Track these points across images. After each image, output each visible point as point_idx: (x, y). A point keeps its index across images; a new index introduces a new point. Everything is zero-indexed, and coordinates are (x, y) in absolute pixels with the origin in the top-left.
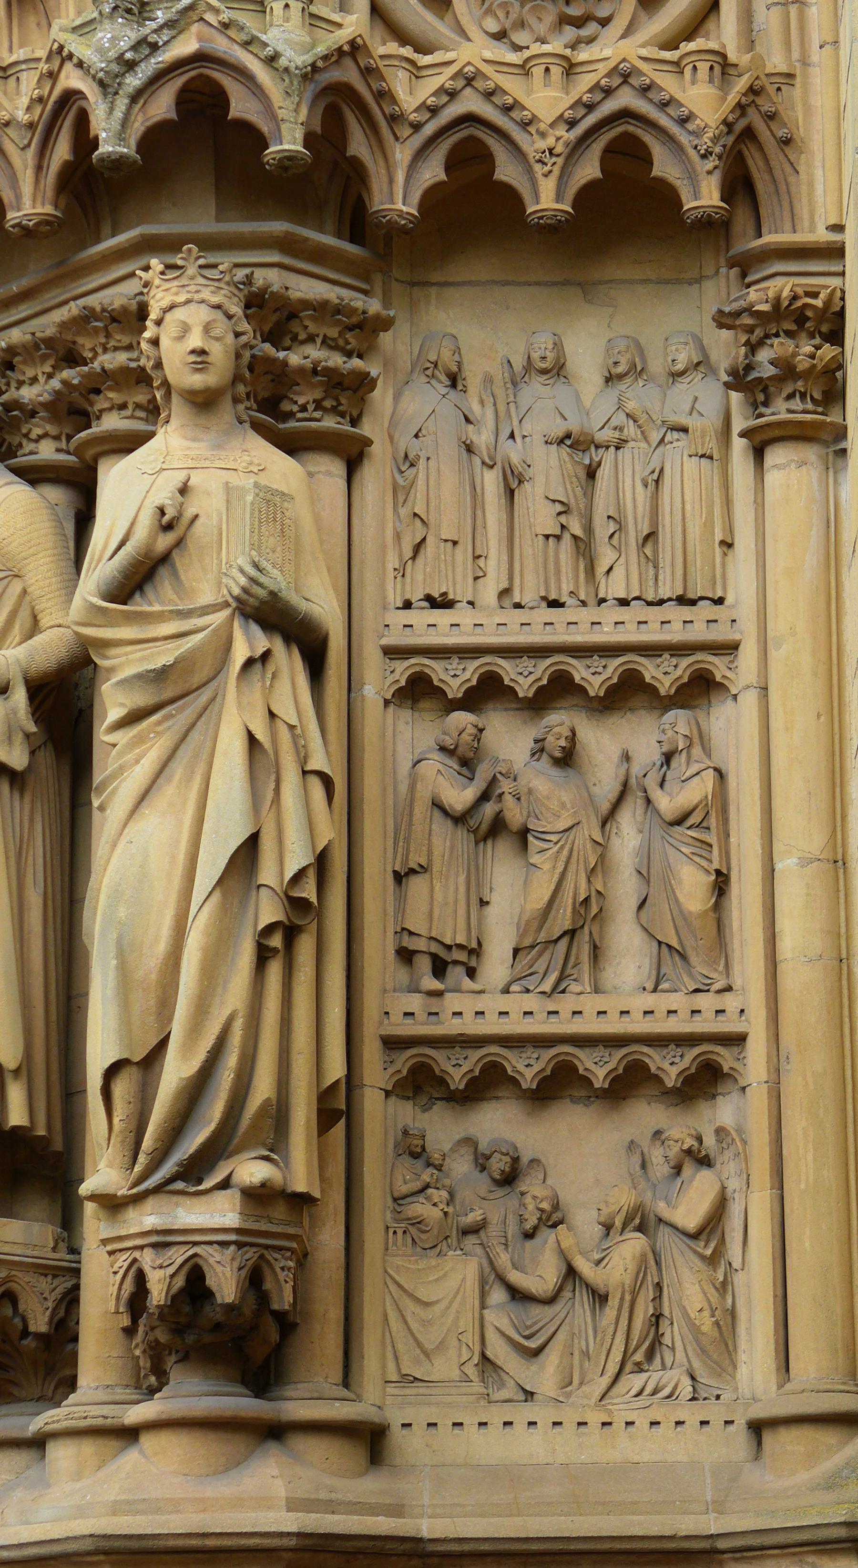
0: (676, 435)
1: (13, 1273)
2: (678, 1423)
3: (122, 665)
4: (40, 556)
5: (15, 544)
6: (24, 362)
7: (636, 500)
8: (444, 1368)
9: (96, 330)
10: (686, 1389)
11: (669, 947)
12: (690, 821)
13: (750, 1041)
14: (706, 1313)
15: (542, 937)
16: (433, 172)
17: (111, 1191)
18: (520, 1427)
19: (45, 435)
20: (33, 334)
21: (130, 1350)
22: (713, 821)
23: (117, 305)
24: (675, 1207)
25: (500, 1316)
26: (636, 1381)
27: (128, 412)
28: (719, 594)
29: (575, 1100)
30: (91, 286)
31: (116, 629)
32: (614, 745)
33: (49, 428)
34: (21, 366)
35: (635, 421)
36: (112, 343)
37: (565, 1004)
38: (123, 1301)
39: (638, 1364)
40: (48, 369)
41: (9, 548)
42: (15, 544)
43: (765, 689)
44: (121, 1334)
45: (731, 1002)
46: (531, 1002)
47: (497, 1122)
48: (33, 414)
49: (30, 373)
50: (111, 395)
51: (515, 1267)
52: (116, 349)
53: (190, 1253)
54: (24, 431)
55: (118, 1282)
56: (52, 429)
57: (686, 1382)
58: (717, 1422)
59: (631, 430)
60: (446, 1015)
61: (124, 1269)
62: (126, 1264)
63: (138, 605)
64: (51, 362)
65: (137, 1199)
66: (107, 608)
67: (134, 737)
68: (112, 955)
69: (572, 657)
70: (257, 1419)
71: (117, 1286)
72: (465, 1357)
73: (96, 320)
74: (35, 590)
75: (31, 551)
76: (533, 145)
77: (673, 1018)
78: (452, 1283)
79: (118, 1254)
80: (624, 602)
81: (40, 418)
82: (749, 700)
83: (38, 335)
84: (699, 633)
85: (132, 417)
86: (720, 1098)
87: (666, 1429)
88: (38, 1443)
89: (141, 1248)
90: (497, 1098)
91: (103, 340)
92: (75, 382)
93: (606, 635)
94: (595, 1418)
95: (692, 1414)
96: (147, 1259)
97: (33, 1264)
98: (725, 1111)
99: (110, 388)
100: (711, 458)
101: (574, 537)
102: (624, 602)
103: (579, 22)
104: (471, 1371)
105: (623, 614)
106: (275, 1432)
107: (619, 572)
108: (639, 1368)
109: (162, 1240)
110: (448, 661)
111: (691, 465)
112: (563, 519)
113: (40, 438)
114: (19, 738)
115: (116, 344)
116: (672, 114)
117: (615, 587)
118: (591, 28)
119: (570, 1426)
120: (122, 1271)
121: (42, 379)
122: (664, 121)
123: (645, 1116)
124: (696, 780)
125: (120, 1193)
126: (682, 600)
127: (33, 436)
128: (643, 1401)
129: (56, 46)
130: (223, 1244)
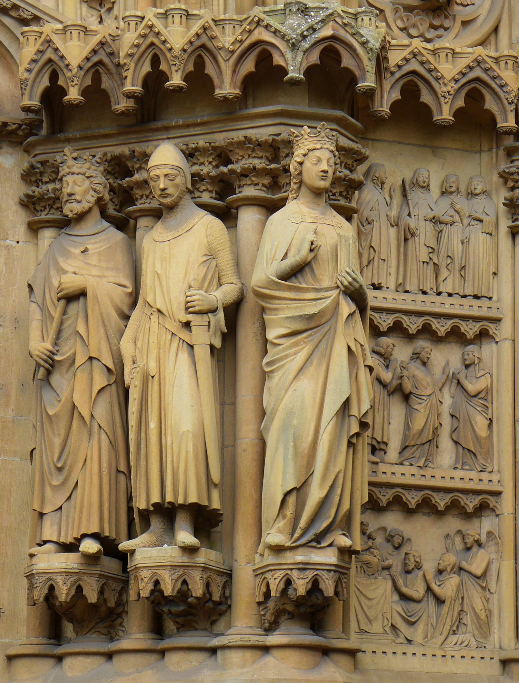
0: (476, 222)
1: (186, 571)
2: (472, 657)
3: (282, 309)
4: (225, 250)
5: (215, 244)
6: (200, 155)
7: (457, 248)
8: (377, 627)
9: (248, 148)
10: (474, 643)
11: (468, 450)
12: (480, 396)
13: (504, 495)
14: (483, 611)
15: (419, 442)
16: (396, 95)
17: (283, 544)
18: (409, 655)
19: (207, 190)
20: (210, 143)
21: (259, 611)
22: (490, 396)
23: (263, 138)
24: (471, 565)
25: (399, 607)
26: (454, 639)
27: (257, 187)
28: (491, 296)
29: (424, 514)
30: (243, 126)
31: (282, 292)
32: (446, 358)
33: (209, 187)
34: (199, 157)
35: (458, 214)
36: (254, 155)
37: (428, 472)
38: (278, 592)
39: (454, 631)
40: (211, 160)
41: (213, 245)
42: (215, 244)
43: (514, 341)
44: (256, 605)
45: (495, 477)
46: (414, 470)
47: (392, 521)
48: (203, 180)
49: (201, 160)
50: (253, 179)
51: (406, 586)
52: (255, 157)
53: (315, 573)
54: (197, 187)
55: (277, 583)
56: (210, 188)
57: (473, 639)
58: (487, 658)
59: (457, 218)
60: (379, 473)
61: (281, 578)
62: (282, 576)
63: (293, 282)
65: (291, 549)
66: (280, 283)
67: (293, 343)
68: (291, 440)
69: (433, 318)
70: (320, 645)
71: (276, 585)
72: (385, 624)
73: (249, 143)
74: (222, 266)
75: (222, 248)
76: (440, 89)
77: (471, 482)
78: (380, 591)
79: (277, 571)
80: (450, 295)
81: (206, 182)
82: (507, 346)
83: (212, 144)
84: (484, 312)
85: (260, 190)
86: (483, 518)
87: (399, 655)
88: (213, 651)
89: (291, 569)
90: (392, 510)
91: (250, 153)
92: (238, 171)
93: (447, 309)
94: (439, 653)
95: (419, 651)
96: (295, 574)
97: (218, 571)
98: (487, 524)
99: (253, 176)
100: (491, 234)
101: (434, 263)
102: (450, 295)
103: (436, 28)
104: (388, 629)
105: (450, 300)
106: (326, 652)
107: (450, 281)
108: (454, 633)
109: (304, 567)
110: (381, 314)
111: (483, 237)
112: (431, 255)
113: (204, 190)
114: (219, 333)
115: (256, 155)
116: (497, 82)
117: (447, 287)
118: (441, 32)
119: (429, 656)
120: (279, 579)
121: (206, 164)
122: (494, 85)
123: (453, 524)
124: (483, 377)
125: (286, 545)
126: (476, 297)
127: (201, 189)
128: (457, 647)
130: (329, 571)
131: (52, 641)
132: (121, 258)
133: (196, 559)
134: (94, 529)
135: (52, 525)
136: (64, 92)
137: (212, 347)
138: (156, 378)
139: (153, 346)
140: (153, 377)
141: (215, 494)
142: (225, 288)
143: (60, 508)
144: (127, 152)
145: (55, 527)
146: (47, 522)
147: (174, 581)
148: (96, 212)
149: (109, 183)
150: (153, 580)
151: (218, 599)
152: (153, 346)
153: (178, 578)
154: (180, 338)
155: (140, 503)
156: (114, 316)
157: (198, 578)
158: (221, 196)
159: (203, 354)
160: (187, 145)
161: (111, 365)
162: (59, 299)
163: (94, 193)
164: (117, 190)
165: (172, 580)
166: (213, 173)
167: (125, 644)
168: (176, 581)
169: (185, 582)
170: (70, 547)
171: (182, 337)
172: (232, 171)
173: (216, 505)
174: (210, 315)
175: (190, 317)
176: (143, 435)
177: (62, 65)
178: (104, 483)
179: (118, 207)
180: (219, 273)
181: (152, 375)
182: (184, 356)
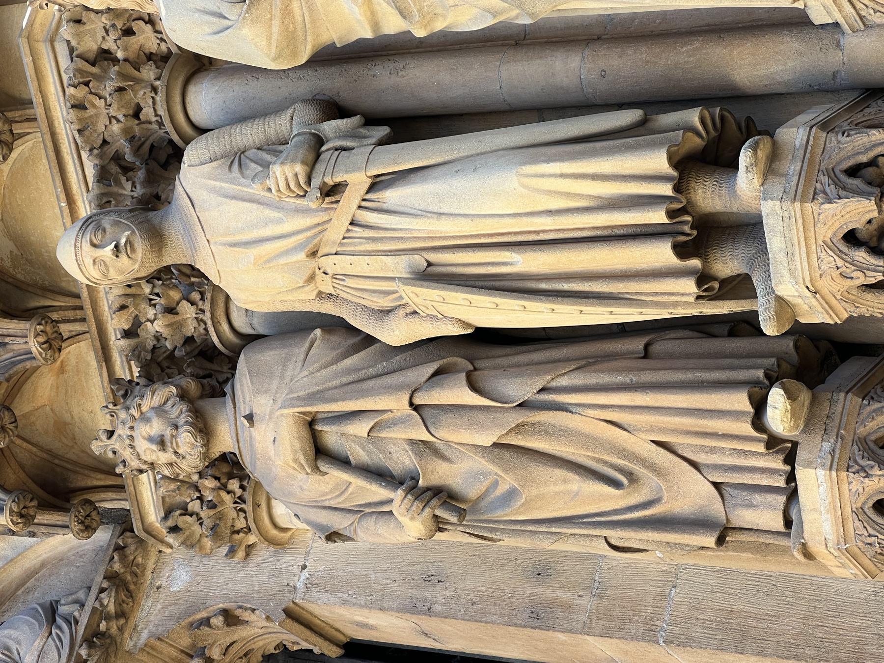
64: (123, 179)
114: (363, 131)
133: (798, 144)
134: (740, 401)
135: (751, 506)
138: (433, 257)
140: (430, 264)
143: (716, 485)
144: (123, 343)
145: (758, 498)
146: (745, 517)
147: (842, 193)
150: (845, 249)
153: (837, 183)
154: (360, 207)
157: (844, 139)
165: (840, 198)
168: (844, 189)
169: (854, 171)
171: (356, 202)
176: (543, 286)
178: (654, 379)
180: (274, 144)
181: (425, 264)
182: (391, 196)
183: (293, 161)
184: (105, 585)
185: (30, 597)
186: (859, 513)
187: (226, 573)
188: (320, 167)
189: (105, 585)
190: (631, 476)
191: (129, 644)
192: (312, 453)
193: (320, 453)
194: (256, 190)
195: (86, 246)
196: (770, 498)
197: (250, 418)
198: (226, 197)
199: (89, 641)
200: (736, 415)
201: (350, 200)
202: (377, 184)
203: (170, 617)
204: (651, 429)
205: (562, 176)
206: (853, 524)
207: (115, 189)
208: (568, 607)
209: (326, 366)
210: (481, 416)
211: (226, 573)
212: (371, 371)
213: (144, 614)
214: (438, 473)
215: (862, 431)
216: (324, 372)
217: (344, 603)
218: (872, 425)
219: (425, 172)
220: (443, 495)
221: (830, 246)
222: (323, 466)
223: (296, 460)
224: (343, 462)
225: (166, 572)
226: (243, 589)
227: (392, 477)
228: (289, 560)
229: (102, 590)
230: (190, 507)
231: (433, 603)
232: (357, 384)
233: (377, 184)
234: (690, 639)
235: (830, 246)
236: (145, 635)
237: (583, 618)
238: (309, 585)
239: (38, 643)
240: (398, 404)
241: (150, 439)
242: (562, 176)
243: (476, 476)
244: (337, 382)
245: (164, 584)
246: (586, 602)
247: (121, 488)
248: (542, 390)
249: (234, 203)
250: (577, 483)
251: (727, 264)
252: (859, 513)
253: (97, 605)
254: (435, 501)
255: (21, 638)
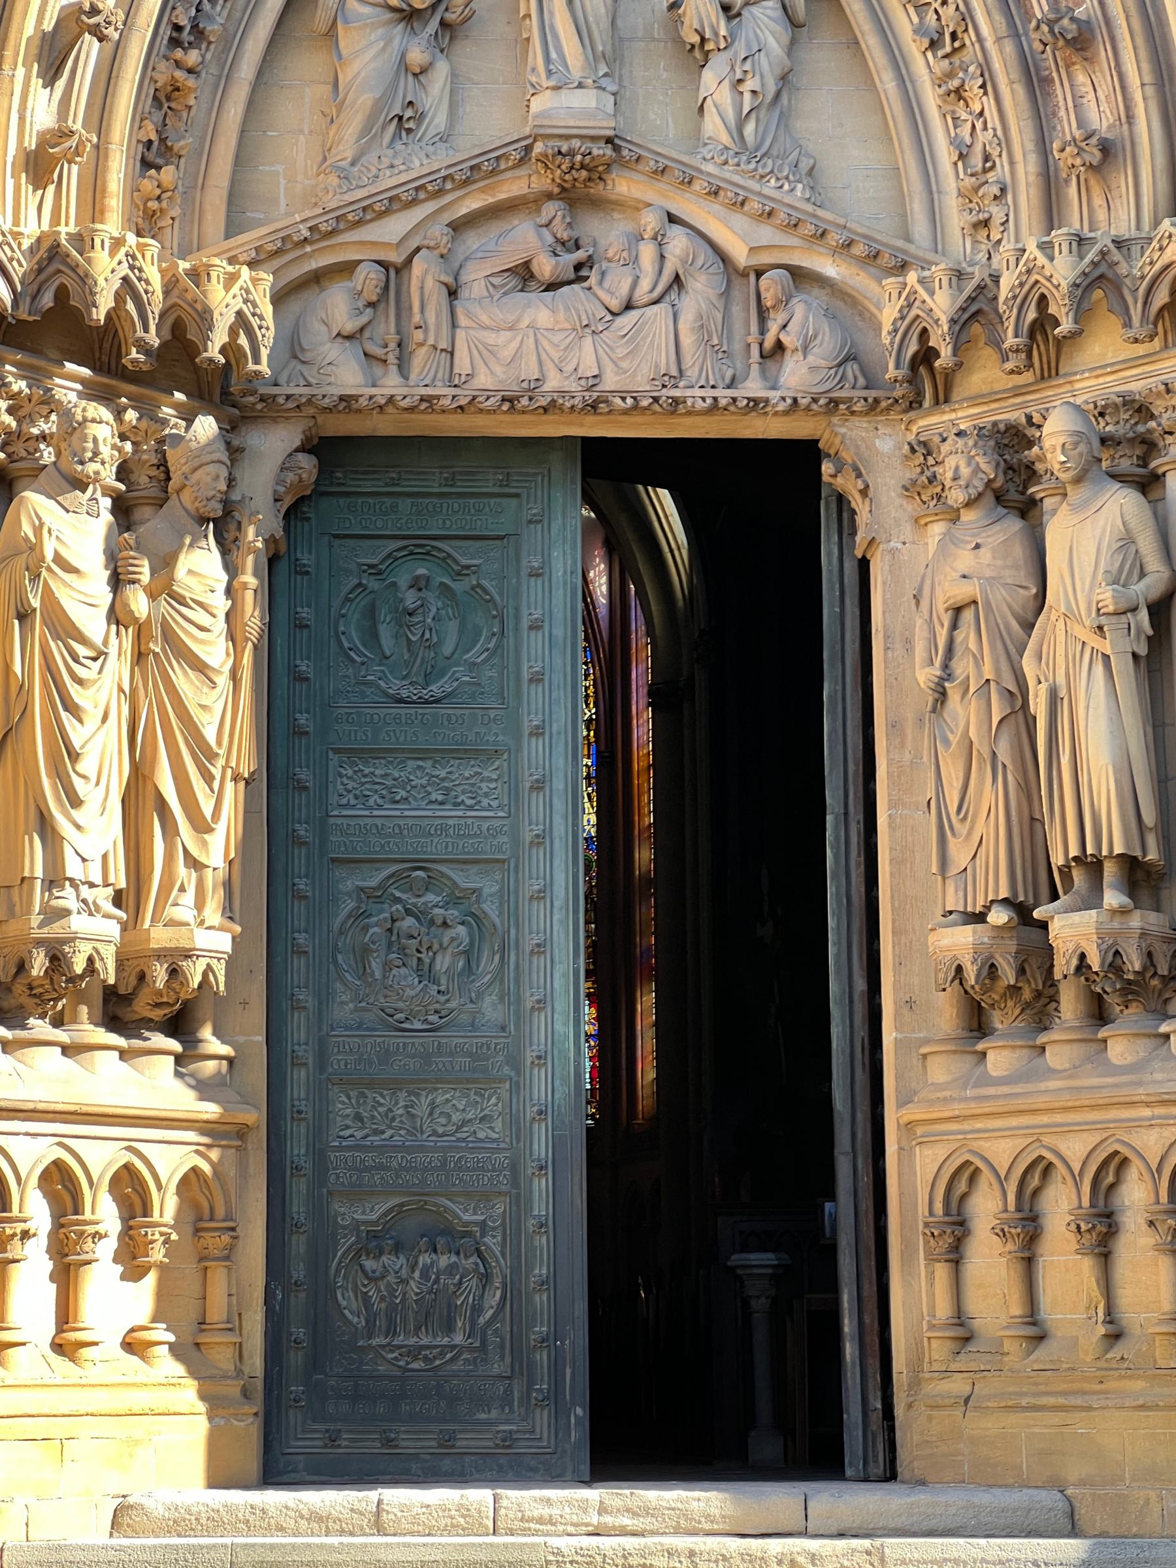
114: (1143, 637)
121: (1122, 423)
129: (1167, 234)
131: (975, 1034)
132: (1019, 551)
134: (1004, 893)
135: (956, 891)
136: (937, 355)
137: (1135, 656)
138: (1066, 701)
139: (1061, 660)
141: (1151, 841)
142: (1146, 581)
145: (961, 894)
146: (951, 888)
148: (989, 498)
149: (1005, 461)
151: (1166, 973)
152: (1061, 660)
153: (1109, 948)
155: (1058, 860)
156: (1015, 625)
158: (1144, 461)
159: (1123, 668)
160: (1095, 403)
161: (1012, 687)
162: (947, 610)
163: (983, 476)
164: (1016, 467)
166: (1131, 435)
167: (1053, 1035)
170: (979, 918)
171: (1096, 647)
172: (1150, 431)
173: (1152, 855)
174: (1129, 615)
175: (1103, 620)
177: (931, 321)
179: (1020, 488)
182: (1099, 669)
183: (1116, 604)
184: (870, 400)
185: (857, 318)
186: (955, 958)
187: (893, 482)
188: (1114, 619)
189: (870, 400)
190: (965, 818)
191: (835, 420)
192: (959, 605)
193: (958, 610)
194: (1100, 577)
195: (1062, 440)
196: (962, 902)
197: (977, 546)
198: (1099, 544)
199: (831, 400)
200: (997, 891)
201: (1094, 641)
202: (1106, 658)
203: (857, 447)
204: (988, 834)
205: (1108, 791)
206: (949, 955)
207: (1122, 410)
208: (902, 745)
209: (1010, 607)
210: (986, 727)
211: (893, 482)
212: (1008, 642)
213: (857, 424)
214: (954, 696)
215: (997, 956)
216: (1006, 609)
217: (884, 583)
218: (1001, 960)
219: (1113, 697)
220: (942, 695)
221: (1078, 946)
222: (950, 612)
223: (949, 598)
224: (954, 626)
225: (888, 431)
226: (884, 499)
227: (950, 659)
228: (907, 529)
229: (866, 400)
230: (929, 458)
231: (893, 649)
232: (998, 635)
233: (1106, 658)
234: (894, 829)
235: (1078, 946)
236: (843, 430)
237: (897, 758)
238: (893, 552)
239: (823, 363)
240: (988, 672)
241: (957, 468)
242: (1108, 791)
243: (955, 718)
244: (999, 621)
245: (880, 432)
246: (908, 757)
247: (937, 403)
248: (1004, 766)
249: (1095, 550)
250: (958, 785)
251: (1078, 875)
252: (955, 958)
253: (855, 400)
254: (937, 695)
255: (825, 344)
